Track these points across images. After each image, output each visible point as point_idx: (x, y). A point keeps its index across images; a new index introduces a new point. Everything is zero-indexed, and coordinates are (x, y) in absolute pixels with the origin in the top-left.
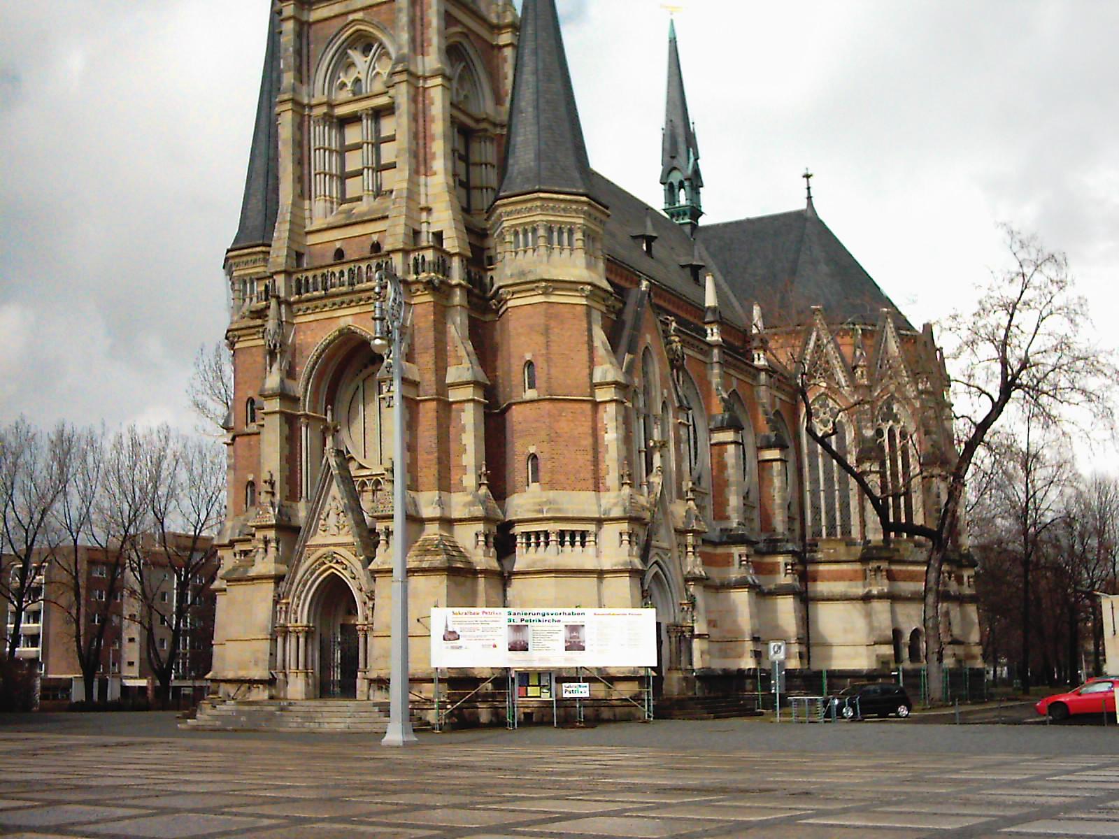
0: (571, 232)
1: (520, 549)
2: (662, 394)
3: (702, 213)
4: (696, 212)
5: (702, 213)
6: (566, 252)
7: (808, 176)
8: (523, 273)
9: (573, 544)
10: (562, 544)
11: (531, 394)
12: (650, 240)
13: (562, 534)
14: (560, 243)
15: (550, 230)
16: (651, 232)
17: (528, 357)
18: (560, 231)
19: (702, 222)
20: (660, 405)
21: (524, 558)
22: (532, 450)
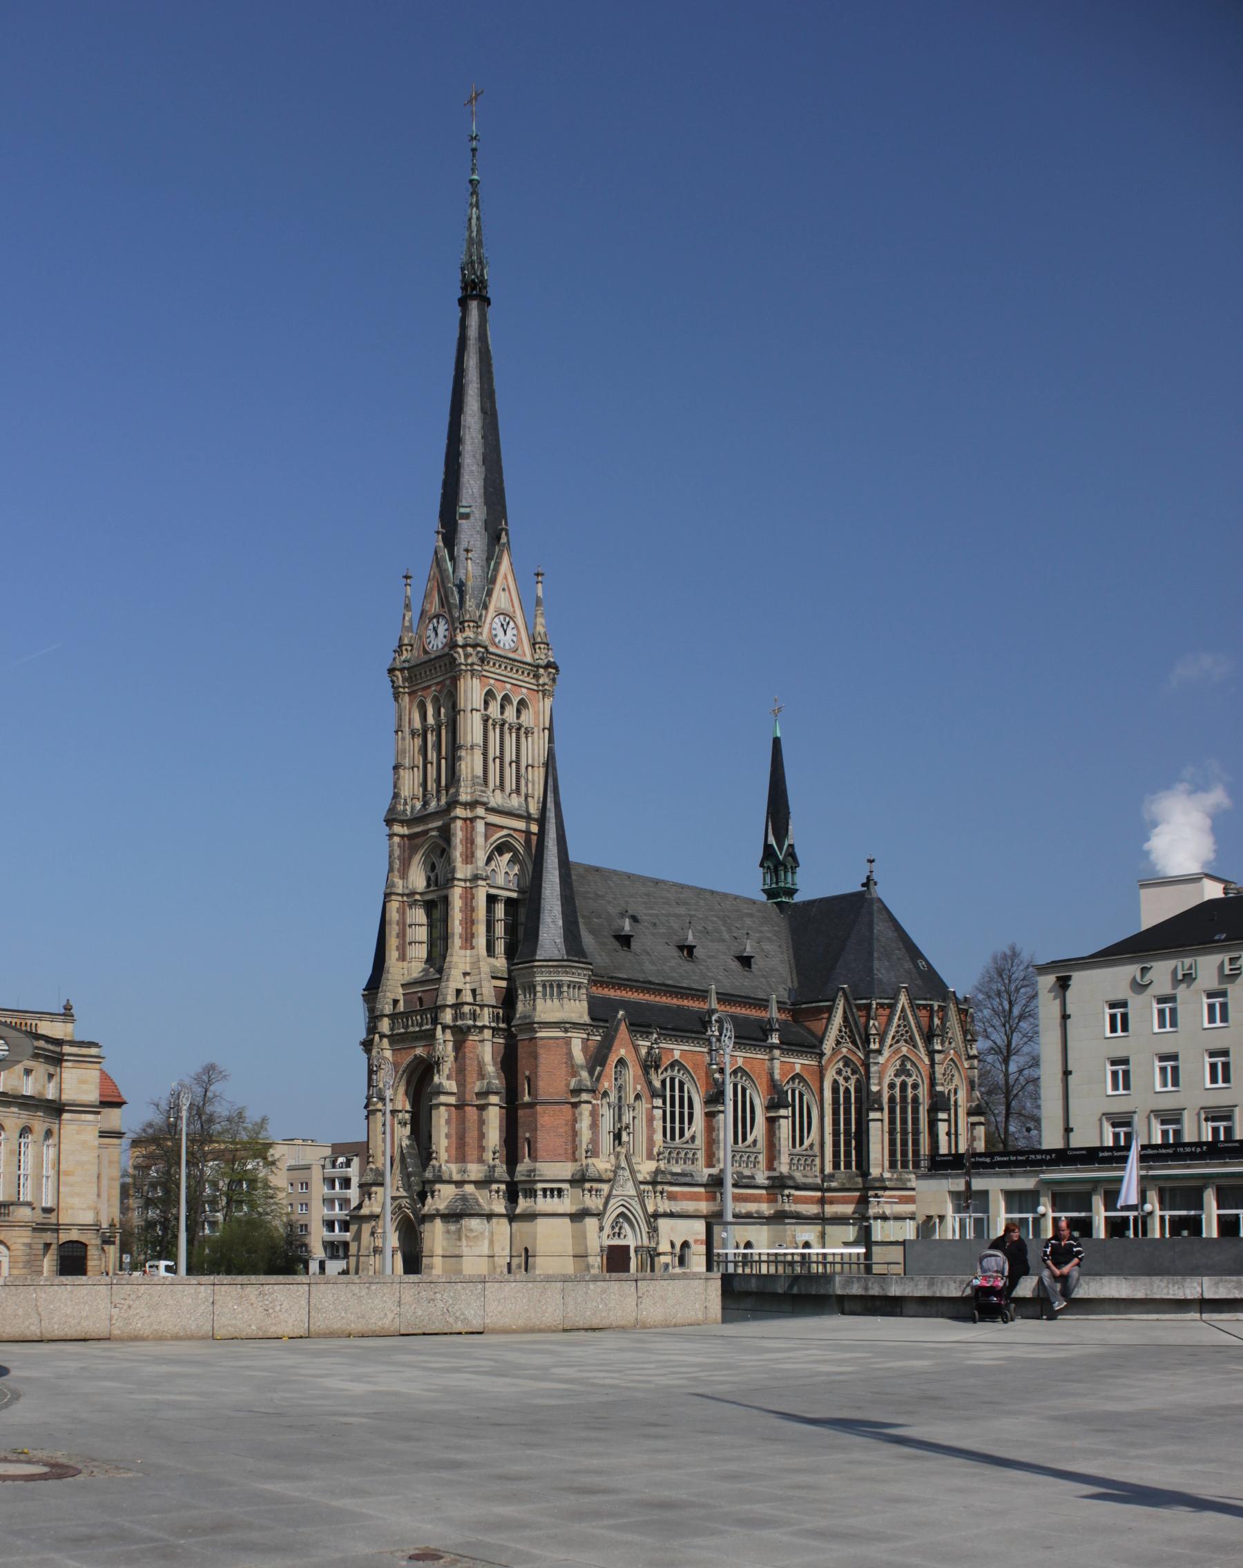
0: (559, 986)
1: (521, 1200)
2: (635, 1089)
3: (797, 890)
4: (791, 892)
5: (797, 890)
6: (556, 1001)
7: (871, 861)
8: (525, 1017)
9: (552, 1196)
10: (545, 1196)
11: (527, 1098)
12: (690, 949)
13: (544, 1190)
14: (552, 995)
15: (544, 986)
16: (691, 940)
17: (527, 1073)
18: (551, 986)
19: (798, 898)
20: (632, 1097)
21: (523, 1204)
22: (527, 1135)
